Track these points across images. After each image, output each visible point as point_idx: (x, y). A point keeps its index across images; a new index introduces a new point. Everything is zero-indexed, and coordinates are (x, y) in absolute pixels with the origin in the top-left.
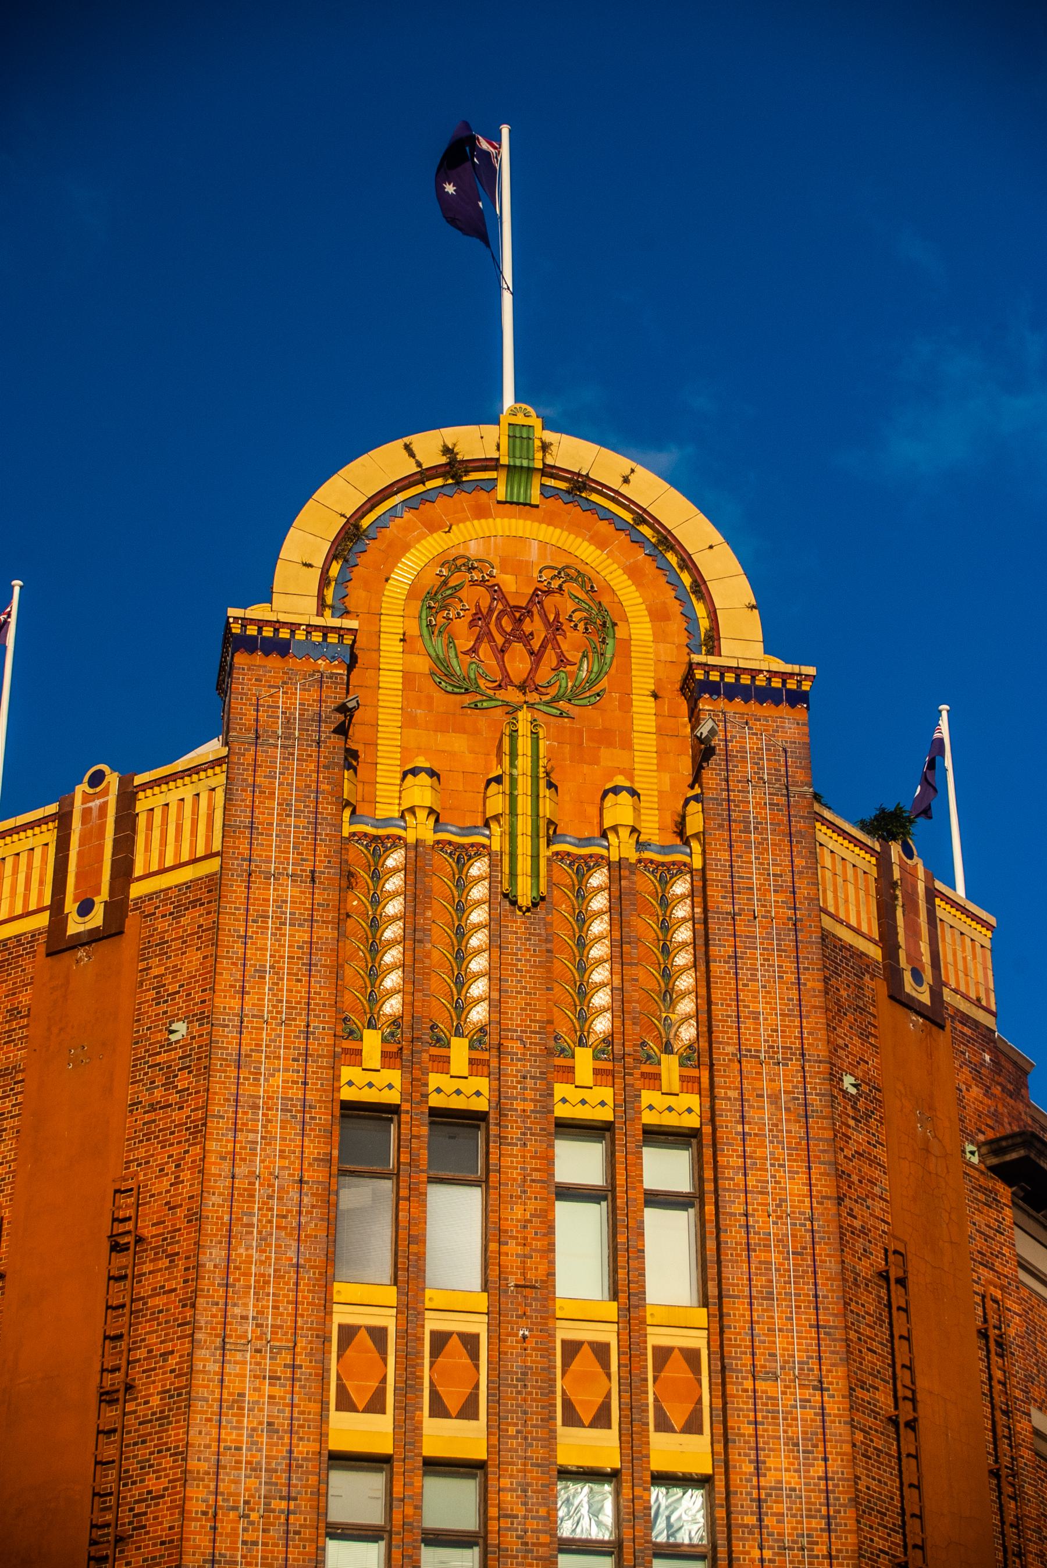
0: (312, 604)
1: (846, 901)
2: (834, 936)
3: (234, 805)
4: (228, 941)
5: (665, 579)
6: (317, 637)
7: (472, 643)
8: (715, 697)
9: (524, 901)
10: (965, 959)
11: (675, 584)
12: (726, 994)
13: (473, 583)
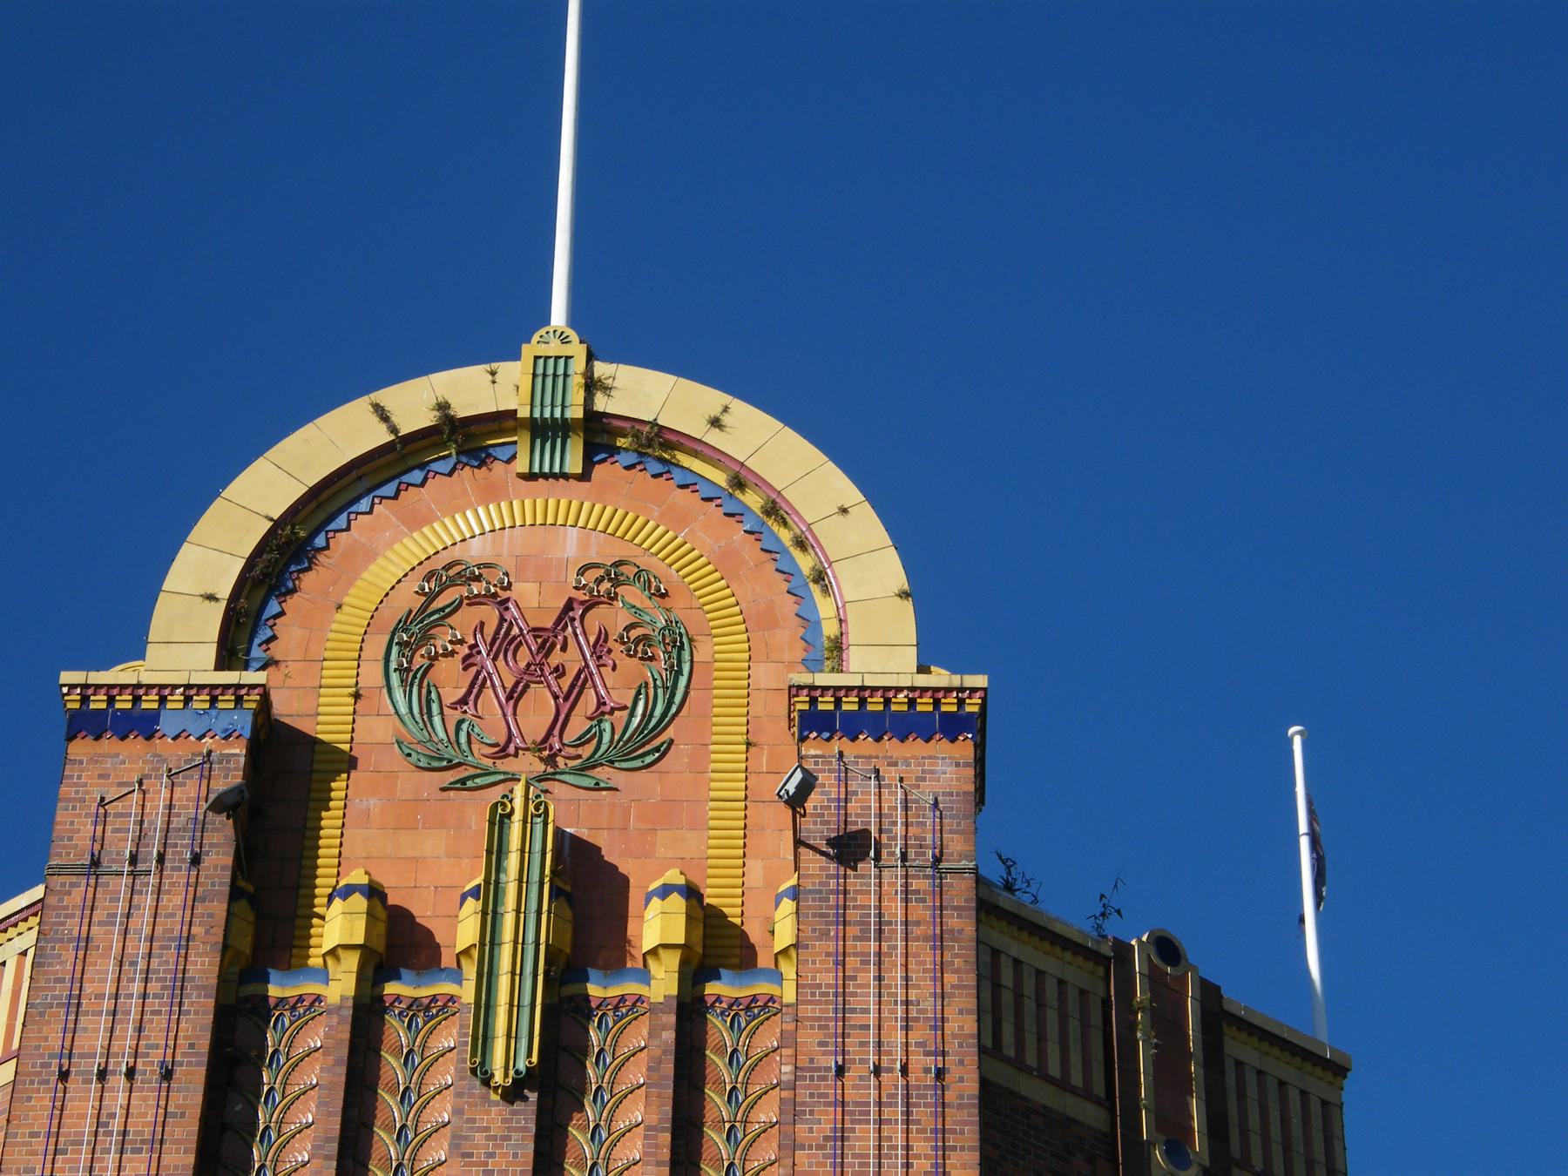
0: (210, 653)
1: (1041, 1040)
2: (1012, 1093)
3: (46, 972)
5: (773, 565)
6: (200, 702)
7: (462, 692)
8: (826, 735)
9: (498, 1078)
10: (1285, 1122)
11: (788, 574)
13: (474, 600)
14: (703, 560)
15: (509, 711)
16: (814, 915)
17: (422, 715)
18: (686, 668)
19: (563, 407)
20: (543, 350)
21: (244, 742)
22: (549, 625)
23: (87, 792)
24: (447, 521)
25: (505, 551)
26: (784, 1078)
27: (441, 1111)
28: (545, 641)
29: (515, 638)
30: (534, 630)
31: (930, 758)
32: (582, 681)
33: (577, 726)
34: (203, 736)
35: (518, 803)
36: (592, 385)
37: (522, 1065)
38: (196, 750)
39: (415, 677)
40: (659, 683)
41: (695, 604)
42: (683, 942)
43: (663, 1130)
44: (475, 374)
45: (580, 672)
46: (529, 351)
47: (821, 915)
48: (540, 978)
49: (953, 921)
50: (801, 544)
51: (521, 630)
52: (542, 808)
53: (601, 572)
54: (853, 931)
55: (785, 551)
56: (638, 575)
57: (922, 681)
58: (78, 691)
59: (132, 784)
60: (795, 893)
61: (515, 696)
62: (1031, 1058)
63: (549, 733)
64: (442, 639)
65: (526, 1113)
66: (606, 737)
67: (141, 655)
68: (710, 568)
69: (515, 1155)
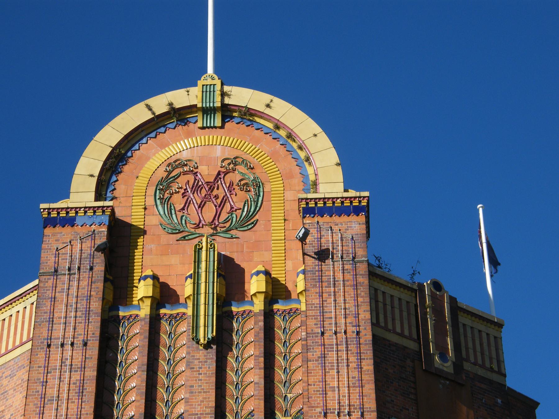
0: (92, 195)
1: (393, 320)
2: (384, 339)
3: (41, 310)
4: (34, 386)
5: (291, 156)
6: (90, 213)
7: (182, 206)
8: (312, 215)
9: (202, 341)
10: (481, 344)
11: (296, 159)
12: (317, 379)
13: (185, 173)
14: (266, 155)
15: (199, 212)
16: (311, 279)
17: (168, 214)
18: (261, 194)
19: (213, 102)
20: (205, 83)
21: (106, 226)
22: (212, 181)
23: (52, 246)
24: (174, 145)
25: (195, 155)
26: (303, 337)
27: (182, 353)
28: (211, 186)
29: (200, 186)
30: (207, 182)
31: (350, 222)
32: (225, 200)
33: (224, 216)
34: (92, 225)
35: (204, 244)
36: (223, 94)
37: (210, 336)
38: (90, 230)
39: (165, 201)
40: (252, 200)
41: (264, 171)
42: (265, 291)
43: (261, 357)
44: (181, 92)
45: (224, 197)
46: (200, 83)
47: (313, 279)
48: (215, 306)
49: (360, 279)
50: (300, 148)
51: (202, 183)
52: (213, 245)
53: (230, 161)
54: (325, 284)
55: (295, 151)
56: (243, 162)
57: (346, 195)
58: (47, 210)
59: (67, 243)
60: (304, 272)
61: (201, 206)
62: (390, 326)
63: (214, 219)
64: (174, 187)
65: (212, 353)
66: (234, 220)
67: (68, 197)
68: (268, 158)
69: (209, 368)
